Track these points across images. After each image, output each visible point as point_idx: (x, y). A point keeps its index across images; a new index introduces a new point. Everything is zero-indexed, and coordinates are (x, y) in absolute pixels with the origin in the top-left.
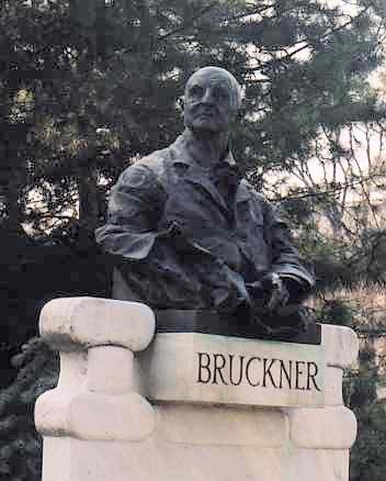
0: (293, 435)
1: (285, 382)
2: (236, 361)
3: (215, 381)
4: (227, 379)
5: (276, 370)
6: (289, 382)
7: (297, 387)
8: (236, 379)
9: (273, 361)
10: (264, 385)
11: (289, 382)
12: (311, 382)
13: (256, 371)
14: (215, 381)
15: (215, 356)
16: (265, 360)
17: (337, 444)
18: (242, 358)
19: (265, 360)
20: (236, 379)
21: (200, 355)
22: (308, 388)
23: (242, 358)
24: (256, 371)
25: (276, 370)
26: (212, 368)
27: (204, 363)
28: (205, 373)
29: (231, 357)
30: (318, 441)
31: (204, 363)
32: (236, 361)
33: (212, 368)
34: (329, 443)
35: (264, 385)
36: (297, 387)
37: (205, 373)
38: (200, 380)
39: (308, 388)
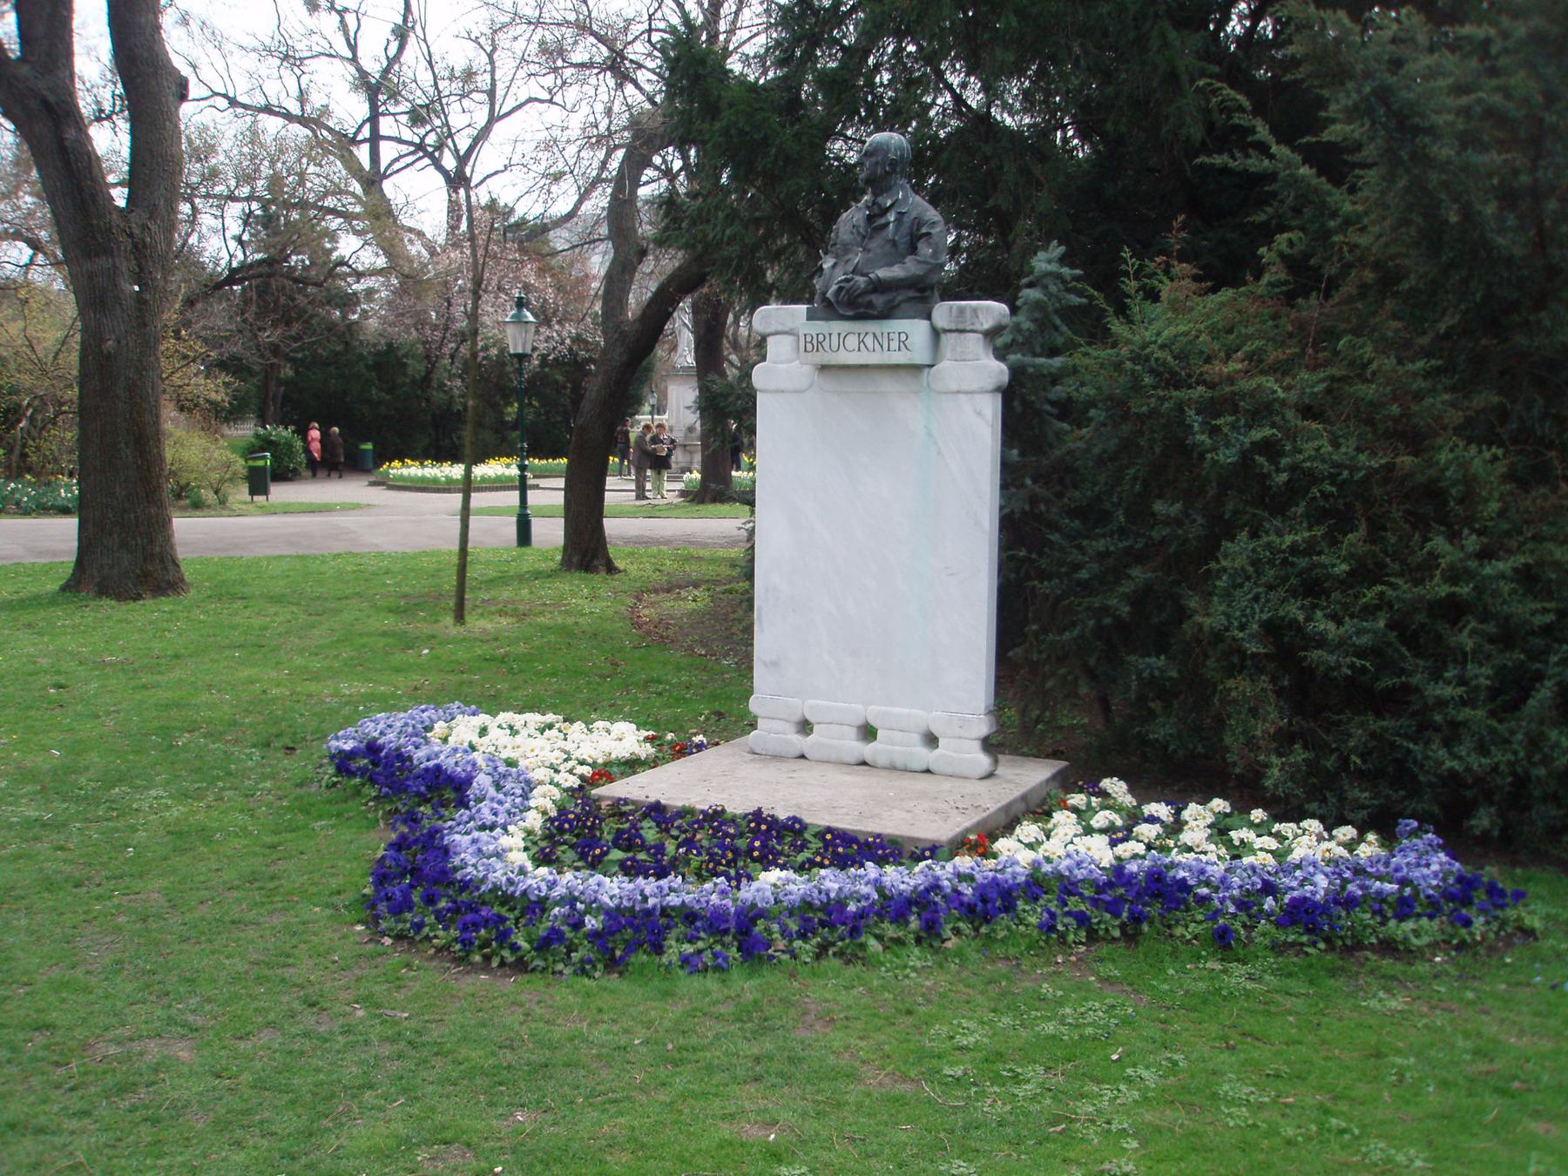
1: (877, 346)
2: (835, 338)
4: (827, 348)
5: (869, 340)
8: (835, 347)
13: (852, 341)
17: (974, 387)
20: (835, 347)
24: (852, 341)
25: (869, 340)
26: (815, 342)
27: (809, 339)
28: (809, 347)
30: (954, 387)
31: (809, 339)
32: (835, 338)
33: (815, 342)
34: (966, 387)
37: (809, 347)
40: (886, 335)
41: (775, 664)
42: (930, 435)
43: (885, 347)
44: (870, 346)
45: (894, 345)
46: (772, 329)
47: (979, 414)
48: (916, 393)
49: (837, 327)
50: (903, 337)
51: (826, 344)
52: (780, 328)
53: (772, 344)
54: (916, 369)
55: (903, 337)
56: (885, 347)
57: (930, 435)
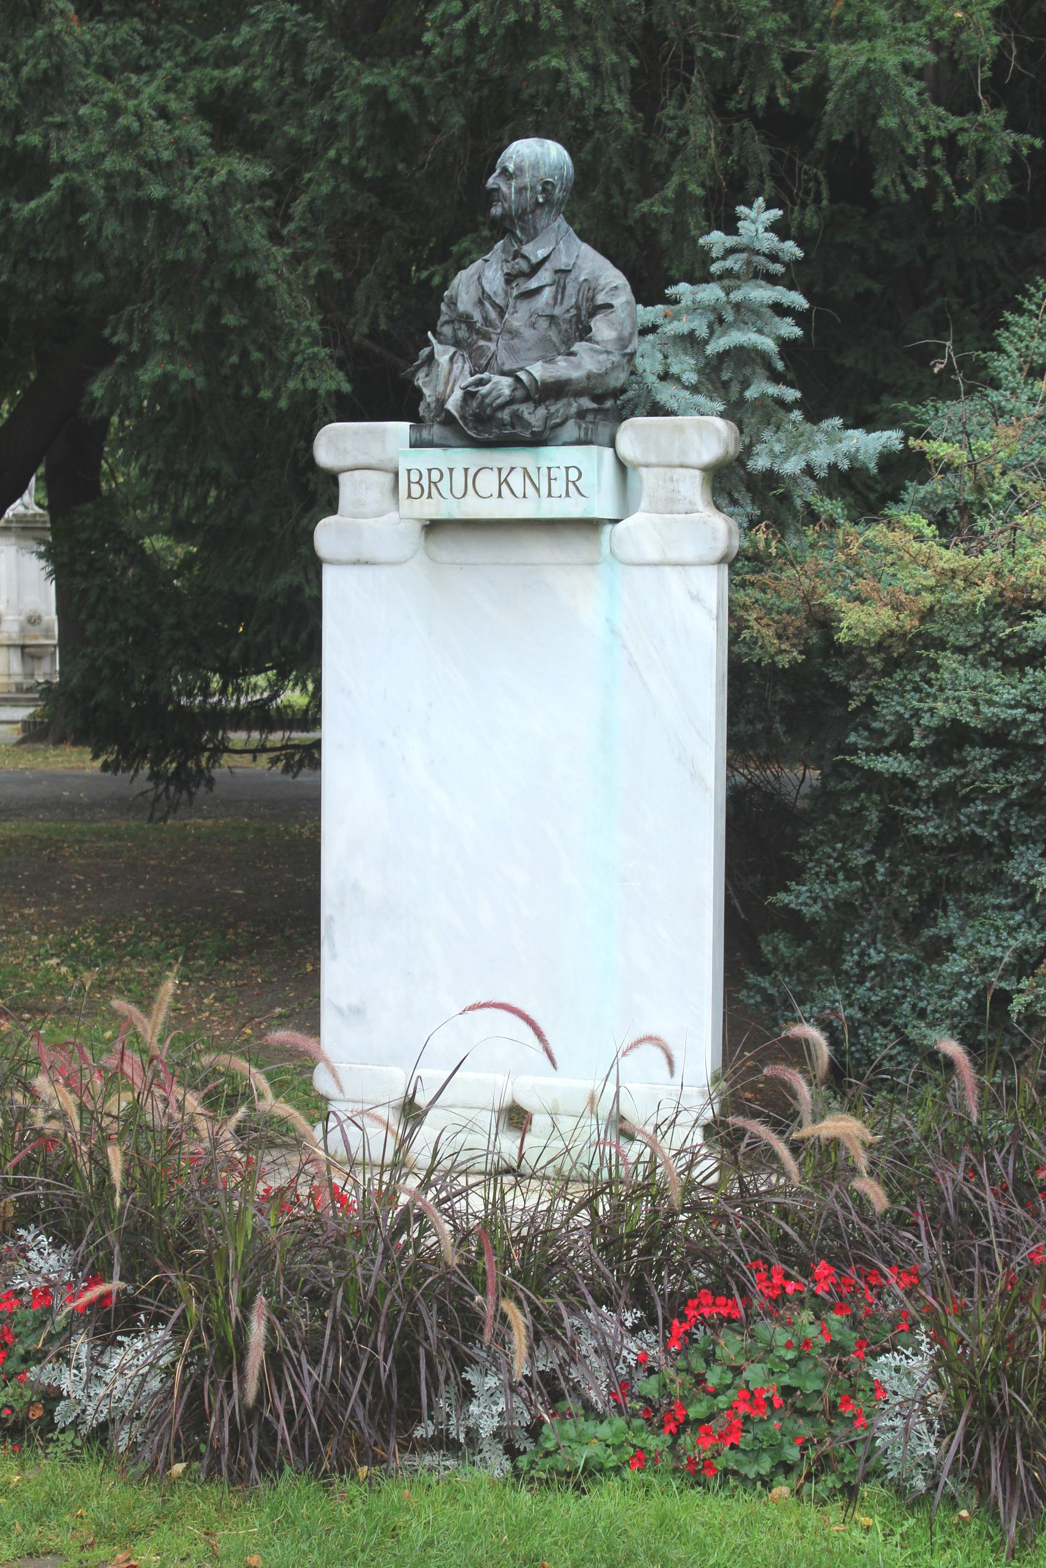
0: (617, 551)
1: (530, 489)
2: (458, 476)
3: (430, 496)
4: (445, 491)
5: (516, 480)
6: (538, 490)
7: (550, 495)
9: (512, 469)
10: (500, 495)
11: (538, 490)
12: (571, 486)
13: (488, 482)
14: (430, 496)
15: (430, 470)
16: (500, 470)
18: (466, 470)
19: (500, 470)
20: (458, 491)
21: (409, 471)
22: (567, 495)
23: (466, 470)
24: (488, 482)
25: (516, 480)
26: (425, 482)
27: (415, 477)
28: (416, 490)
29: (451, 470)
30: (652, 553)
31: (415, 477)
32: (458, 476)
33: (425, 482)
34: (673, 556)
35: (500, 495)
36: (550, 495)
37: (416, 490)
38: (409, 496)
39: (567, 495)
40: (544, 471)
41: (357, 1011)
42: (614, 632)
43: (544, 490)
44: (519, 491)
45: (558, 487)
46: (349, 462)
47: (696, 598)
48: (592, 564)
49: (462, 458)
50: (573, 475)
51: (444, 486)
52: (362, 460)
53: (348, 486)
54: (591, 526)
55: (573, 475)
56: (544, 490)
57: (614, 632)
